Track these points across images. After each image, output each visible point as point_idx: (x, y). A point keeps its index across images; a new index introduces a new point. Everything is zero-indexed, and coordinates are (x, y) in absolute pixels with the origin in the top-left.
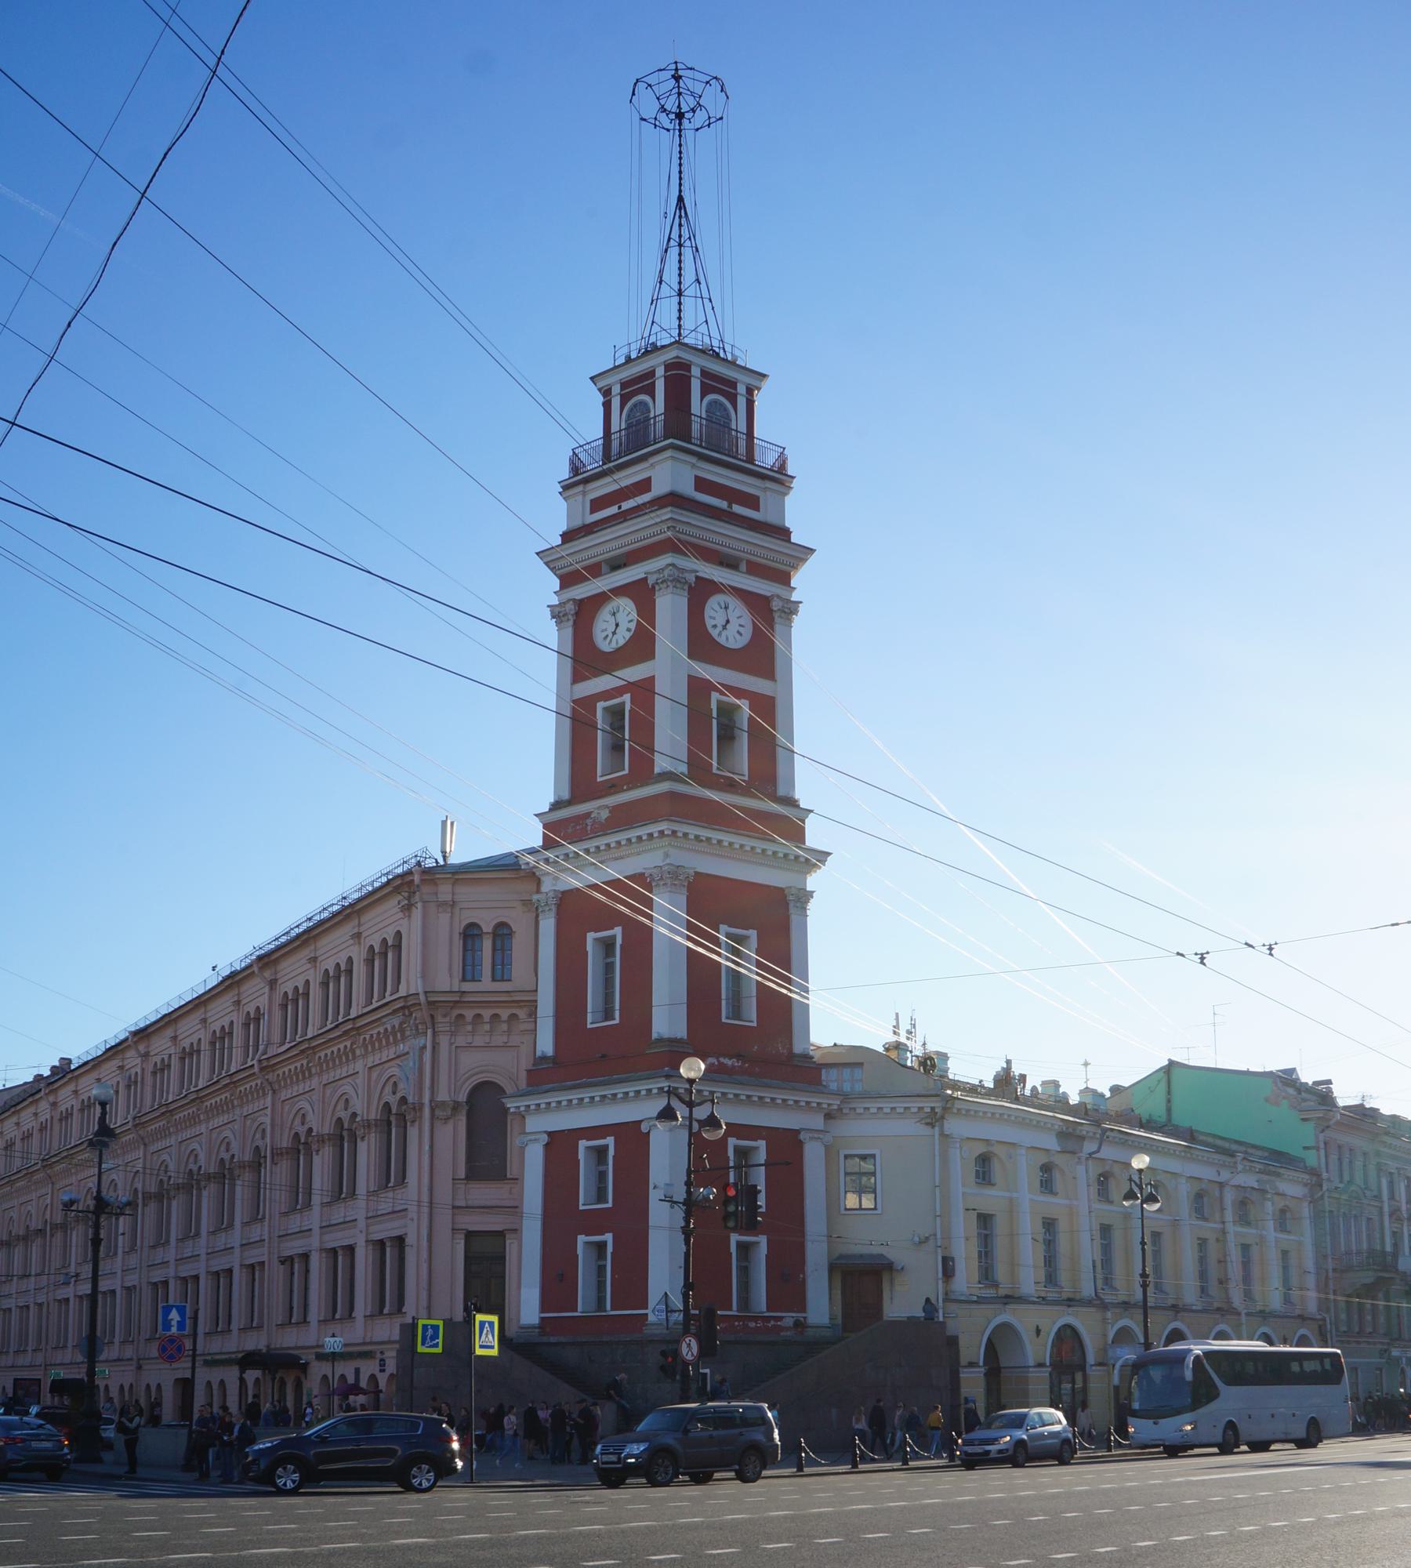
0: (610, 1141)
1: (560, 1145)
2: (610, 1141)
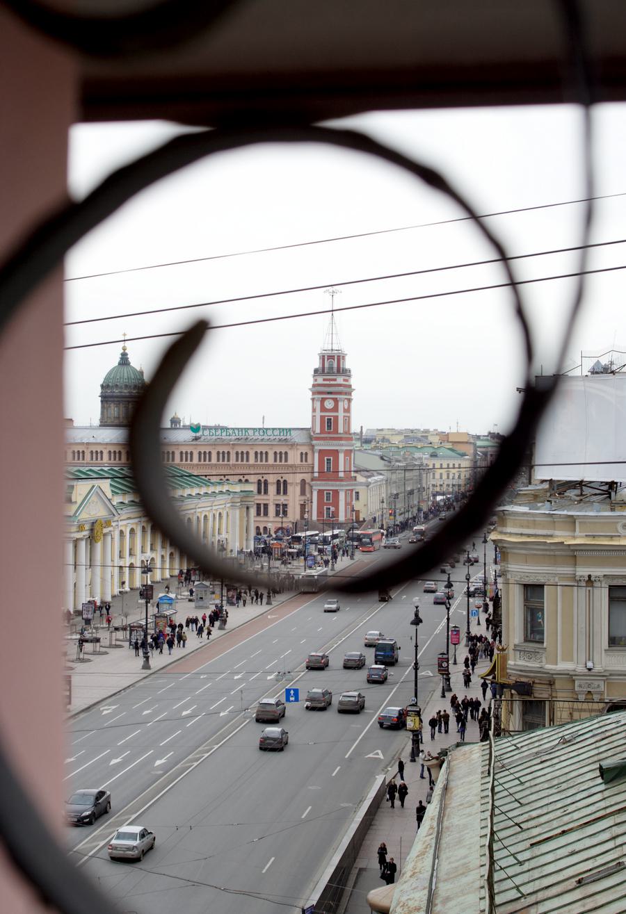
0: (331, 492)
1: (320, 492)
2: (331, 492)
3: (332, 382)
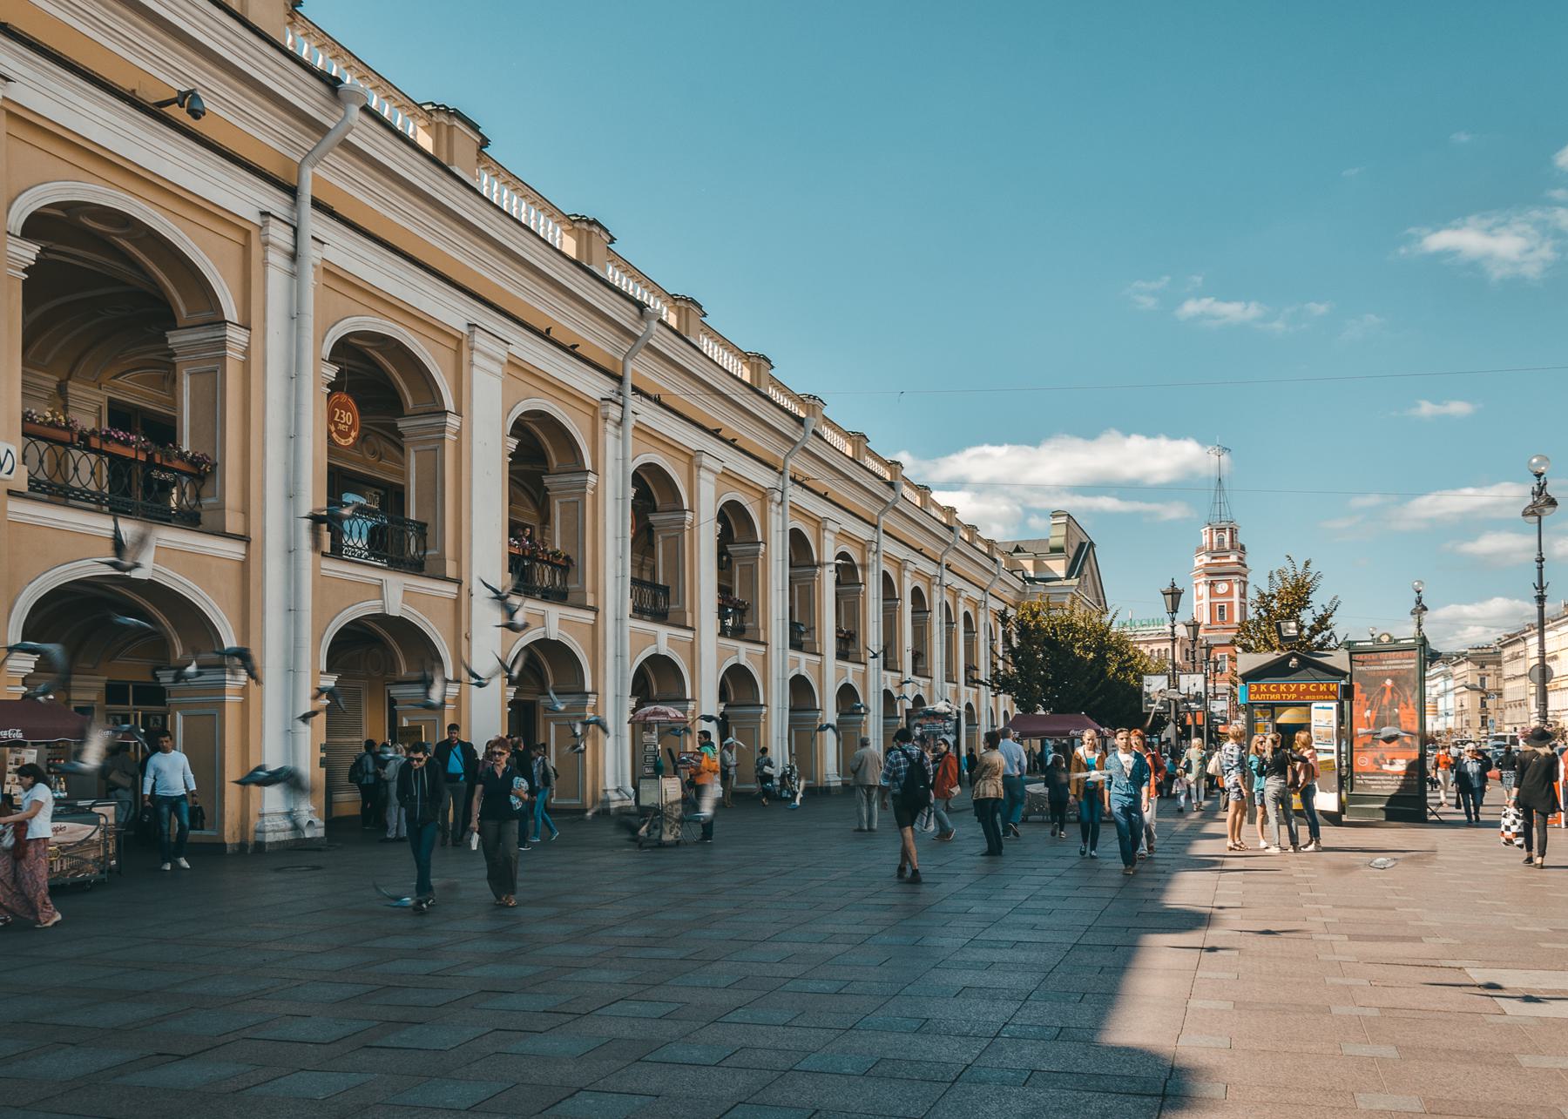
3: (1223, 561)
